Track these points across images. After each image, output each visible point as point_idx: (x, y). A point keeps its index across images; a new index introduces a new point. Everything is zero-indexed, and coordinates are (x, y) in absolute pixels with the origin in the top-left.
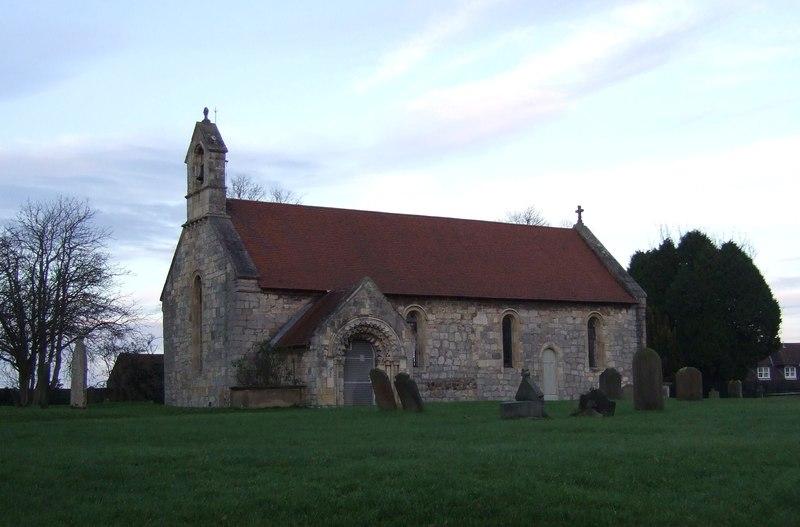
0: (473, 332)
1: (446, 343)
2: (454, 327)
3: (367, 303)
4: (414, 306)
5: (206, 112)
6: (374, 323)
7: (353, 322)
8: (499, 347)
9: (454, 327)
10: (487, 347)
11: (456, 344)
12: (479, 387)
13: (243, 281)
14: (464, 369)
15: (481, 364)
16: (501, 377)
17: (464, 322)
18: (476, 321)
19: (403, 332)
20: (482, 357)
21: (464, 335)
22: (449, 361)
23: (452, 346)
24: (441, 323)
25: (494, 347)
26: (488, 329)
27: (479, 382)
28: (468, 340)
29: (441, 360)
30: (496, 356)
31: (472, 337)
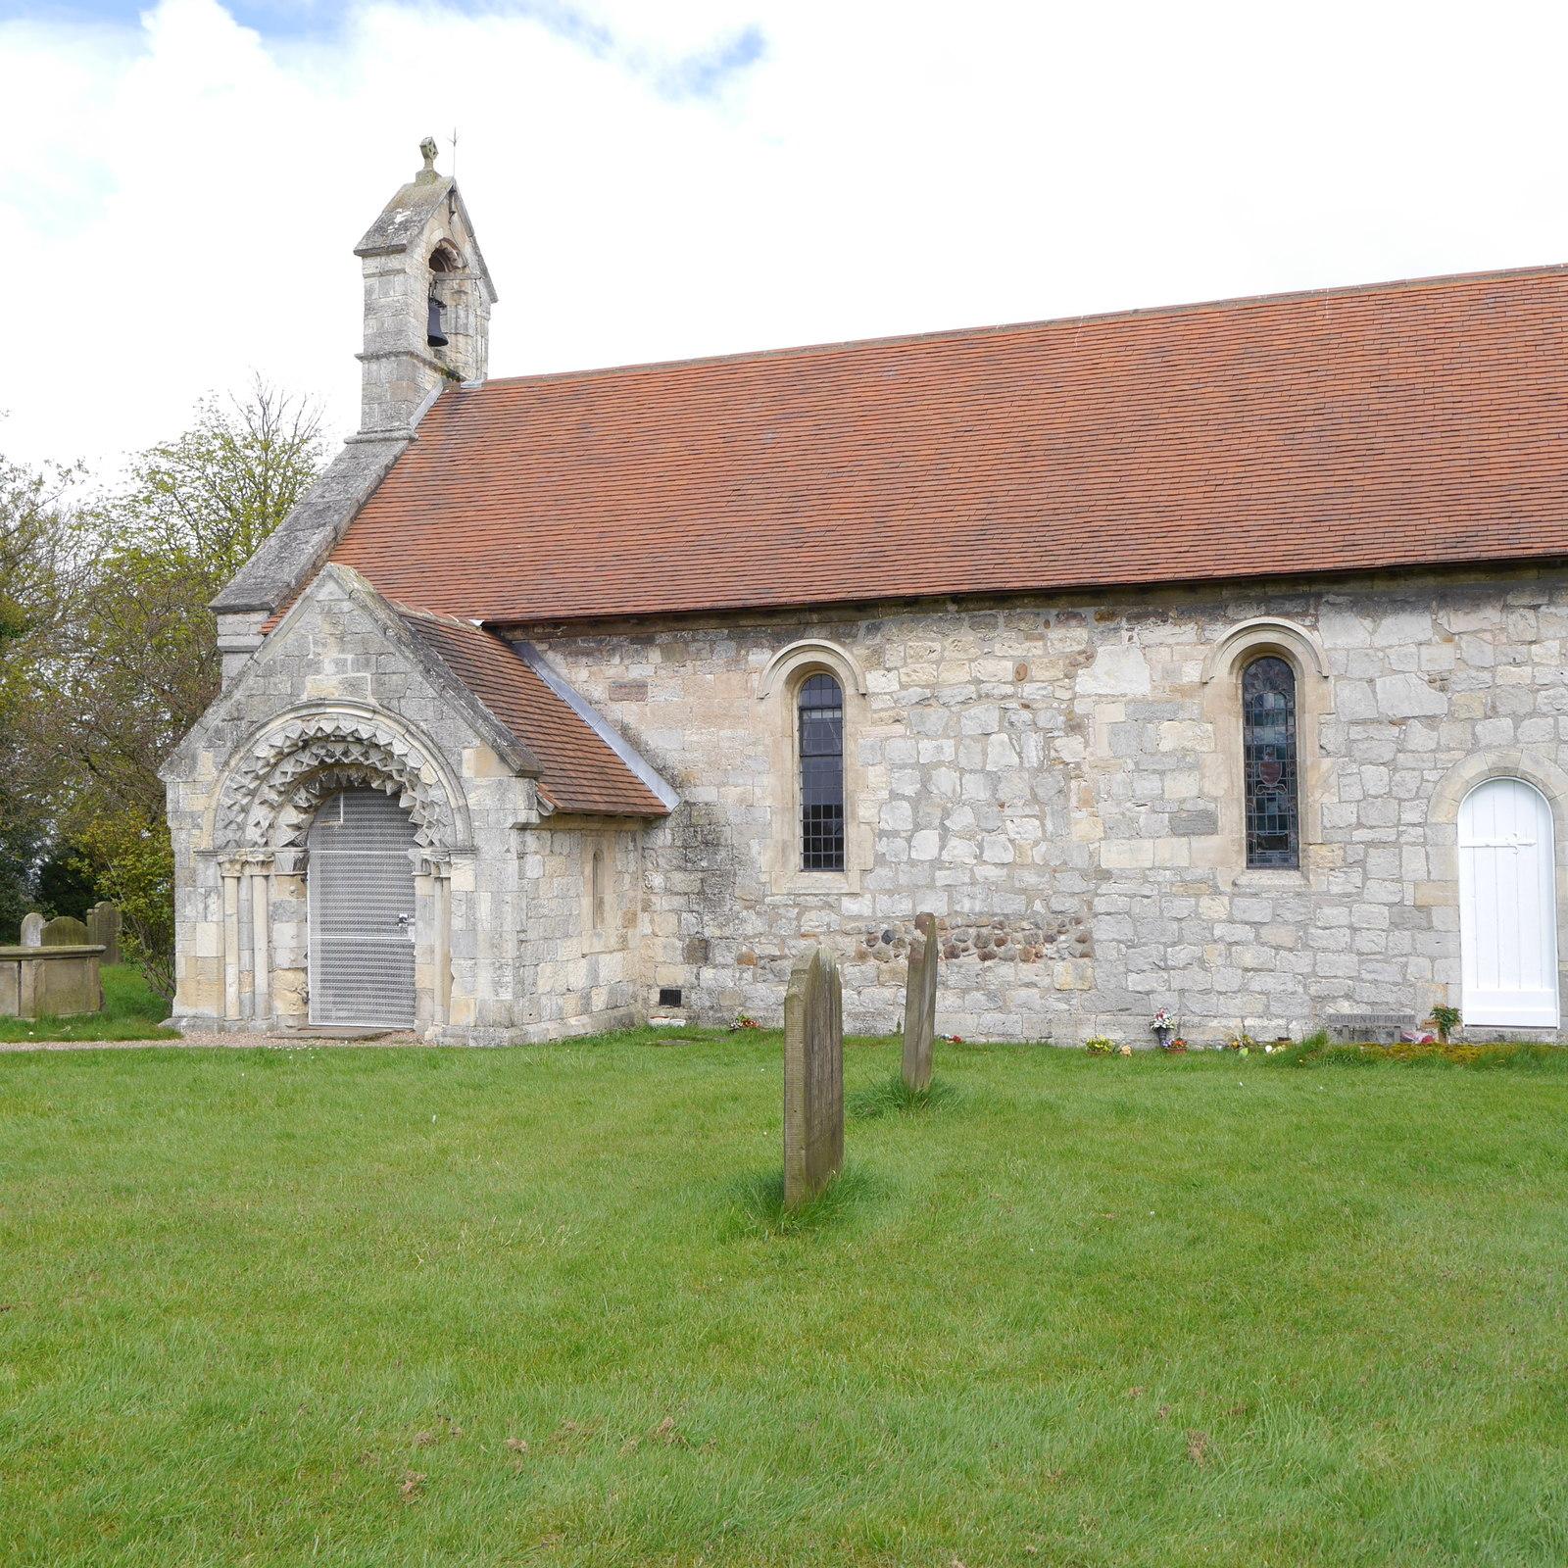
0: (1075, 726)
1: (944, 781)
2: (985, 715)
3: (330, 656)
4: (817, 647)
5: (428, 150)
6: (347, 726)
7: (280, 731)
8: (1223, 784)
9: (985, 715)
10: (1148, 786)
11: (994, 780)
12: (1105, 951)
13: (230, 618)
14: (1030, 878)
15: (1114, 856)
16: (1214, 908)
17: (1028, 690)
18: (1086, 682)
19: (467, 754)
20: (1124, 829)
21: (1032, 744)
22: (960, 850)
23: (975, 789)
24: (923, 702)
25: (1182, 787)
26: (1145, 712)
27: (1104, 931)
28: (1051, 762)
29: (927, 844)
30: (1197, 823)
31: (1070, 748)
